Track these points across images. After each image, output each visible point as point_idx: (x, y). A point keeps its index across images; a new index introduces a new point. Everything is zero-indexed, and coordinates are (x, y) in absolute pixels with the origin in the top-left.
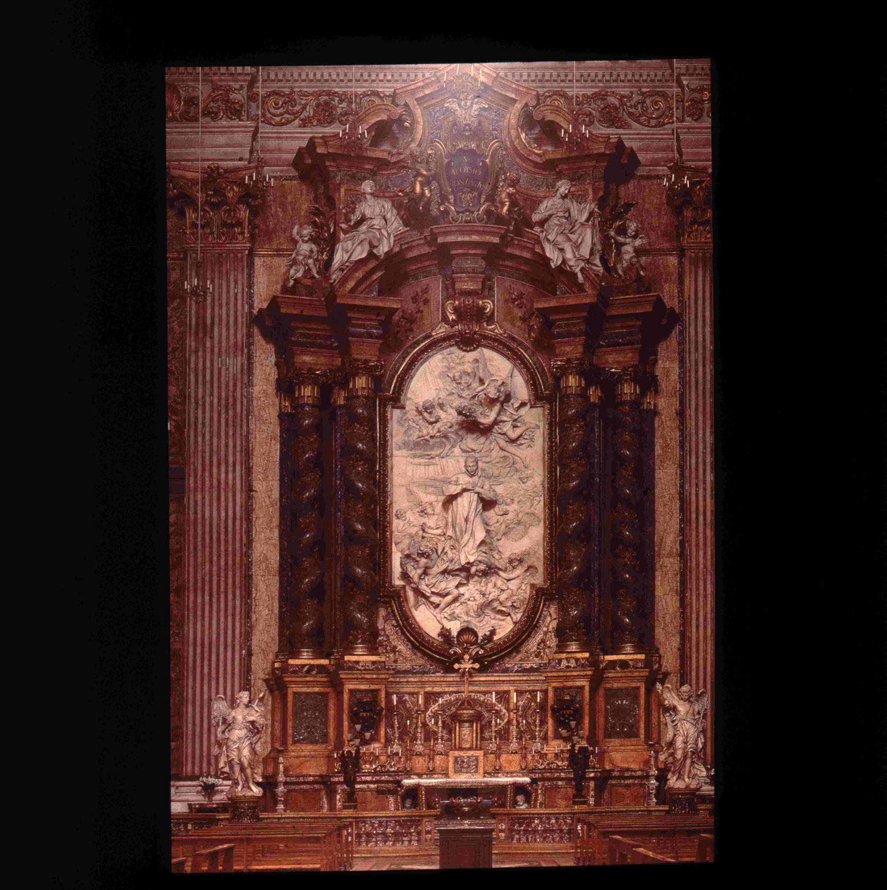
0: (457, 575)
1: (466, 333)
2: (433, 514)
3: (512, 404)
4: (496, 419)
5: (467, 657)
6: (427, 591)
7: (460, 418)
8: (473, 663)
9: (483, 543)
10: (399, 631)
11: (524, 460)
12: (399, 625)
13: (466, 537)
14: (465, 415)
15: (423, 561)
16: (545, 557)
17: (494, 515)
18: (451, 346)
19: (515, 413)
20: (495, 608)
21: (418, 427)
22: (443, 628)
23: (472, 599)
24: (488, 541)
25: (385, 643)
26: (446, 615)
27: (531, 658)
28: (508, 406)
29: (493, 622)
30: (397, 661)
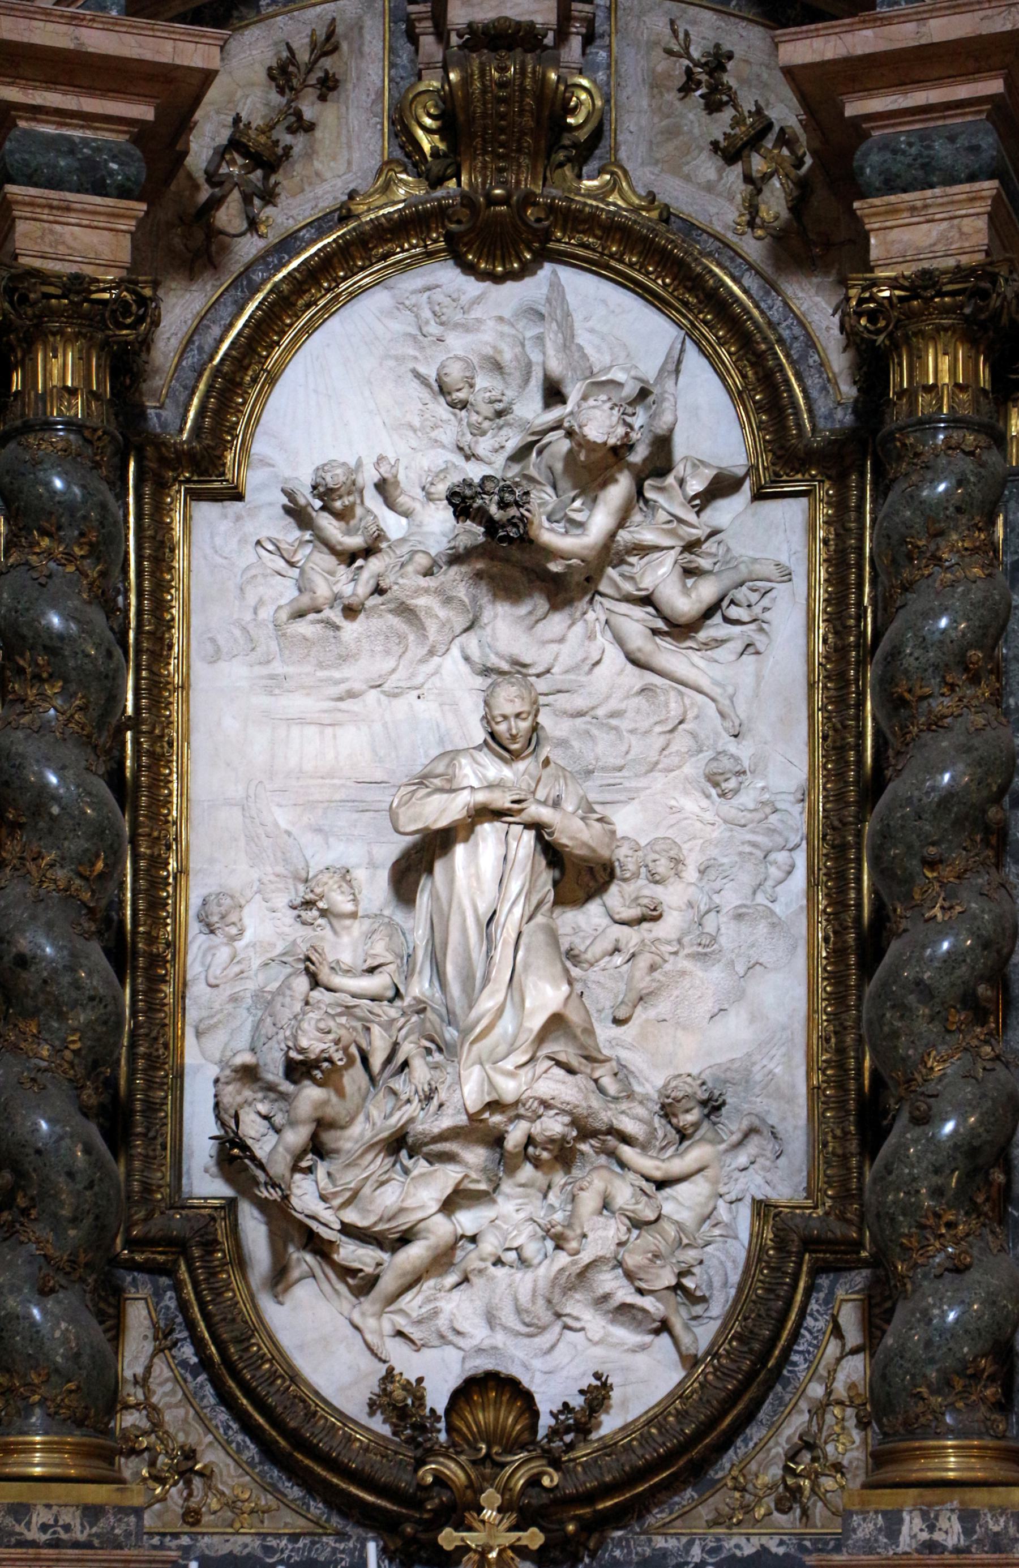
0: (449, 1158)
1: (492, 201)
2: (353, 915)
3: (682, 482)
5: (491, 1498)
7: (474, 532)
10: (209, 1390)
12: (205, 1363)
13: (488, 1002)
14: (482, 516)
15: (311, 1094)
16: (814, 1092)
17: (606, 921)
19: (691, 517)
20: (606, 1297)
21: (295, 572)
22: (390, 1376)
23: (512, 1256)
24: (574, 1016)
26: (401, 1322)
27: (760, 1512)
29: (598, 1351)
30: (197, 1512)
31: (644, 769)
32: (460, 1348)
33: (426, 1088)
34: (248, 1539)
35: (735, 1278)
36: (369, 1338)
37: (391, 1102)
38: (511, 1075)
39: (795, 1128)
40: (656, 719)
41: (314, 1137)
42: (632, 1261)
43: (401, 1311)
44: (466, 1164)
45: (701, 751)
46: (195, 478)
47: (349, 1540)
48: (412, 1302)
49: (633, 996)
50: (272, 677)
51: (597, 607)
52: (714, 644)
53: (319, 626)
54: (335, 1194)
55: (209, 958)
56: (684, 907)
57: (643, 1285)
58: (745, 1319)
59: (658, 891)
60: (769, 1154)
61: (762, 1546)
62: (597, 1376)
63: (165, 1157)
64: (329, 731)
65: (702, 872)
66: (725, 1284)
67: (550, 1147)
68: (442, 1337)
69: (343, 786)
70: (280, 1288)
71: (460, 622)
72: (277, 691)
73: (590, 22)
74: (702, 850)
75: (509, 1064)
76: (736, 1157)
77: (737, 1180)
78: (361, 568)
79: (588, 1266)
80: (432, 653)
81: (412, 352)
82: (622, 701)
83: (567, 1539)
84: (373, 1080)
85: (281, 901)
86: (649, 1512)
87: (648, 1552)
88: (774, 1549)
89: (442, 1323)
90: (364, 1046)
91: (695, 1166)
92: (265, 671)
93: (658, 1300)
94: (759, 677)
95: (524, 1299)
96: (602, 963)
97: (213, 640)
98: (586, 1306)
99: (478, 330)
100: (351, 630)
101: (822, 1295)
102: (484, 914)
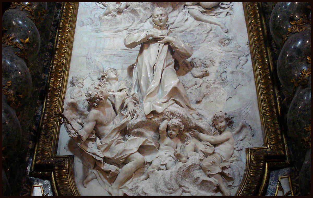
0: (140, 134)
2: (116, 79)
6: (100, 155)
9: (175, 90)
11: (223, 26)
15: (94, 111)
17: (192, 78)
20: (197, 179)
35: (242, 173)
38: (160, 105)
40: (204, 30)
41: (95, 128)
44: (147, 137)
48: (129, 184)
49: (202, 95)
50: (98, 28)
52: (218, 13)
55: (72, 92)
57: (210, 173)
58: (247, 184)
60: (250, 134)
63: (51, 143)
64: (112, 39)
66: (239, 175)
72: (99, 32)
76: (239, 136)
79: (189, 167)
80: (141, 21)
85: (95, 78)
90: (114, 102)
91: (225, 138)
92: (95, 28)
93: (216, 178)
94: (231, 20)
95: (168, 179)
96: (191, 88)
98: (191, 184)
100: (119, 17)
101: (273, 178)
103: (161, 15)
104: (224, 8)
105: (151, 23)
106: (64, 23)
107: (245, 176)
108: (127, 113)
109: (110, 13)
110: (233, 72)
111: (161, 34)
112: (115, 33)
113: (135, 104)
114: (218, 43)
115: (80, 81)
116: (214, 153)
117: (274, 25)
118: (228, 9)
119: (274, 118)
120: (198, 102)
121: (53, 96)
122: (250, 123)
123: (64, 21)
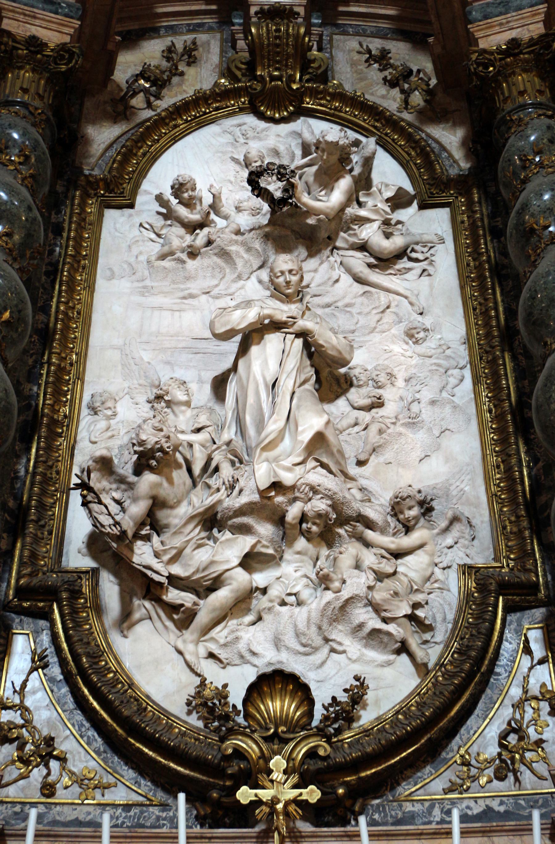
0: (245, 530)
1: (273, 78)
2: (188, 404)
4: (342, 210)
8: (295, 787)
11: (413, 299)
15: (149, 478)
17: (349, 408)
18: (242, 110)
20: (361, 626)
21: (161, 241)
25: (15, 733)
27: (483, 780)
28: (368, 195)
31: (367, 331)
32: (255, 666)
33: (231, 479)
34: (91, 809)
35: (451, 616)
36: (188, 657)
37: (206, 493)
38: (289, 469)
39: (482, 522)
40: (373, 306)
42: (378, 596)
43: (212, 639)
44: (259, 535)
45: (401, 322)
46: (107, 194)
47: (170, 810)
49: (369, 448)
50: (145, 287)
51: (335, 255)
52: (404, 271)
53: (173, 263)
54: (165, 551)
55: (92, 428)
56: (398, 400)
58: (462, 639)
59: (380, 391)
60: (467, 536)
61: (487, 806)
62: (357, 678)
63: (51, 539)
65: (407, 380)
66: (444, 619)
67: (318, 521)
68: (242, 657)
69: (184, 340)
70: (125, 625)
71: (256, 263)
72: (147, 294)
73: (321, 36)
74: (406, 370)
75: (287, 463)
76: (445, 539)
77: (446, 554)
78: (197, 234)
80: (239, 277)
81: (230, 149)
82: (352, 299)
83: (339, 799)
84: (194, 485)
85: (142, 399)
86: (399, 784)
87: (400, 815)
88: (497, 808)
89: (242, 646)
90: (188, 457)
93: (399, 625)
94: (431, 287)
95: (302, 626)
97: (110, 269)
98: (346, 635)
99: (266, 139)
100: (191, 264)
102: (270, 381)
103: (290, 271)
104: (417, 260)
105: (260, 282)
106: (72, 272)
107: (456, 622)
108: (219, 482)
109: (172, 253)
110: (433, 402)
111: (290, 315)
112: (184, 301)
113: (233, 463)
114: (403, 336)
115: (109, 404)
116: (395, 573)
117: (529, 315)
118: (425, 262)
119: (518, 504)
120: (360, 463)
121: (53, 435)
122: (466, 511)
123: (72, 266)
